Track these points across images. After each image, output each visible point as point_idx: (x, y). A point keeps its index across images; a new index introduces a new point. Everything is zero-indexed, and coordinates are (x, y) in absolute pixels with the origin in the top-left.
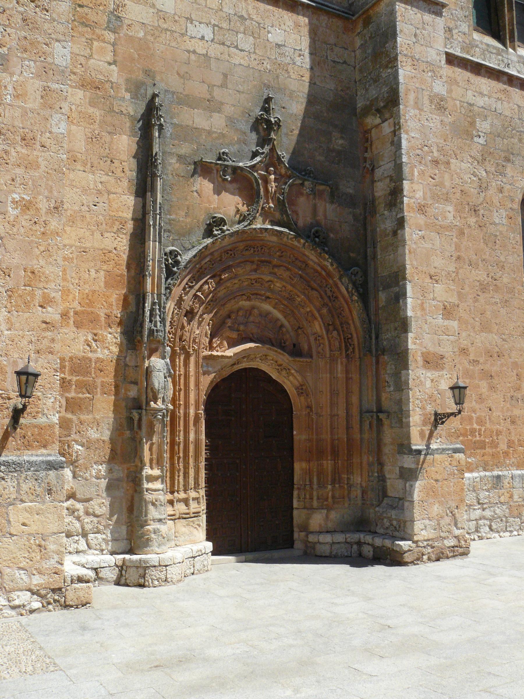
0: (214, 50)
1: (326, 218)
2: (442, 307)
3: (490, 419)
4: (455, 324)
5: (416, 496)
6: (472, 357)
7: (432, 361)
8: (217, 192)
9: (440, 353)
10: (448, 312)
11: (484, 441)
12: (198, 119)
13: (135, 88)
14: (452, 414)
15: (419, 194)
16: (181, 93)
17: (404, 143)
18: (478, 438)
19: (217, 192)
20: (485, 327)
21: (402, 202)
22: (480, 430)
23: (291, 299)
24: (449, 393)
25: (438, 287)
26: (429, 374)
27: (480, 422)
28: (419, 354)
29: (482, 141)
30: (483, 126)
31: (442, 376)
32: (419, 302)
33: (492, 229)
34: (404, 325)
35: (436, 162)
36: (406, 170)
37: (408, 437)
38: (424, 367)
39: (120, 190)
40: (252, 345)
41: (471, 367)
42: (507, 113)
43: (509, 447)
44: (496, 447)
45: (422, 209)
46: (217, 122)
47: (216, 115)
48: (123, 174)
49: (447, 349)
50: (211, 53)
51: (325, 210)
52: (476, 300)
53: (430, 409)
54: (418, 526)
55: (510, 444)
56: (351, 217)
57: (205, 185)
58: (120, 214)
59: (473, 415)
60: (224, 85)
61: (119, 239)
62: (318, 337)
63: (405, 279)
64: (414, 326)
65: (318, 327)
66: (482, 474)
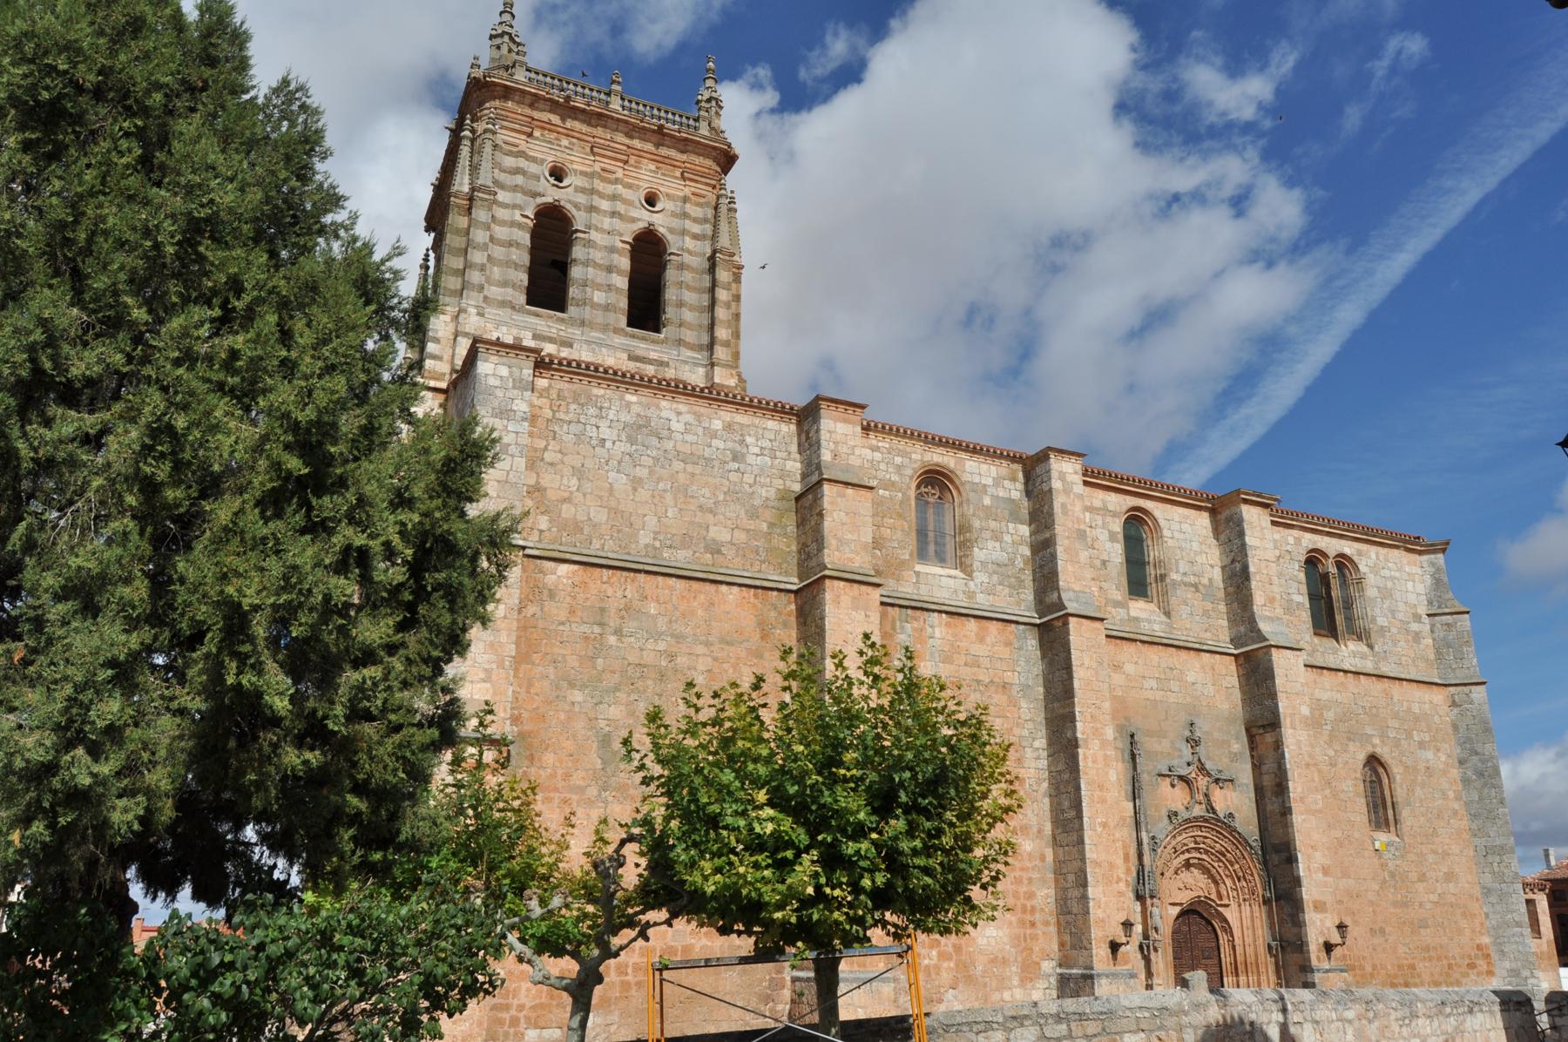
0: (1159, 695)
4: (1329, 879)
7: (1320, 907)
10: (1326, 871)
13: (1120, 729)
25: (1318, 854)
33: (1342, 796)
34: (1297, 882)
35: (1308, 765)
45: (1302, 799)
49: (1328, 899)
53: (1321, 941)
55: (1374, 967)
64: (1304, 882)
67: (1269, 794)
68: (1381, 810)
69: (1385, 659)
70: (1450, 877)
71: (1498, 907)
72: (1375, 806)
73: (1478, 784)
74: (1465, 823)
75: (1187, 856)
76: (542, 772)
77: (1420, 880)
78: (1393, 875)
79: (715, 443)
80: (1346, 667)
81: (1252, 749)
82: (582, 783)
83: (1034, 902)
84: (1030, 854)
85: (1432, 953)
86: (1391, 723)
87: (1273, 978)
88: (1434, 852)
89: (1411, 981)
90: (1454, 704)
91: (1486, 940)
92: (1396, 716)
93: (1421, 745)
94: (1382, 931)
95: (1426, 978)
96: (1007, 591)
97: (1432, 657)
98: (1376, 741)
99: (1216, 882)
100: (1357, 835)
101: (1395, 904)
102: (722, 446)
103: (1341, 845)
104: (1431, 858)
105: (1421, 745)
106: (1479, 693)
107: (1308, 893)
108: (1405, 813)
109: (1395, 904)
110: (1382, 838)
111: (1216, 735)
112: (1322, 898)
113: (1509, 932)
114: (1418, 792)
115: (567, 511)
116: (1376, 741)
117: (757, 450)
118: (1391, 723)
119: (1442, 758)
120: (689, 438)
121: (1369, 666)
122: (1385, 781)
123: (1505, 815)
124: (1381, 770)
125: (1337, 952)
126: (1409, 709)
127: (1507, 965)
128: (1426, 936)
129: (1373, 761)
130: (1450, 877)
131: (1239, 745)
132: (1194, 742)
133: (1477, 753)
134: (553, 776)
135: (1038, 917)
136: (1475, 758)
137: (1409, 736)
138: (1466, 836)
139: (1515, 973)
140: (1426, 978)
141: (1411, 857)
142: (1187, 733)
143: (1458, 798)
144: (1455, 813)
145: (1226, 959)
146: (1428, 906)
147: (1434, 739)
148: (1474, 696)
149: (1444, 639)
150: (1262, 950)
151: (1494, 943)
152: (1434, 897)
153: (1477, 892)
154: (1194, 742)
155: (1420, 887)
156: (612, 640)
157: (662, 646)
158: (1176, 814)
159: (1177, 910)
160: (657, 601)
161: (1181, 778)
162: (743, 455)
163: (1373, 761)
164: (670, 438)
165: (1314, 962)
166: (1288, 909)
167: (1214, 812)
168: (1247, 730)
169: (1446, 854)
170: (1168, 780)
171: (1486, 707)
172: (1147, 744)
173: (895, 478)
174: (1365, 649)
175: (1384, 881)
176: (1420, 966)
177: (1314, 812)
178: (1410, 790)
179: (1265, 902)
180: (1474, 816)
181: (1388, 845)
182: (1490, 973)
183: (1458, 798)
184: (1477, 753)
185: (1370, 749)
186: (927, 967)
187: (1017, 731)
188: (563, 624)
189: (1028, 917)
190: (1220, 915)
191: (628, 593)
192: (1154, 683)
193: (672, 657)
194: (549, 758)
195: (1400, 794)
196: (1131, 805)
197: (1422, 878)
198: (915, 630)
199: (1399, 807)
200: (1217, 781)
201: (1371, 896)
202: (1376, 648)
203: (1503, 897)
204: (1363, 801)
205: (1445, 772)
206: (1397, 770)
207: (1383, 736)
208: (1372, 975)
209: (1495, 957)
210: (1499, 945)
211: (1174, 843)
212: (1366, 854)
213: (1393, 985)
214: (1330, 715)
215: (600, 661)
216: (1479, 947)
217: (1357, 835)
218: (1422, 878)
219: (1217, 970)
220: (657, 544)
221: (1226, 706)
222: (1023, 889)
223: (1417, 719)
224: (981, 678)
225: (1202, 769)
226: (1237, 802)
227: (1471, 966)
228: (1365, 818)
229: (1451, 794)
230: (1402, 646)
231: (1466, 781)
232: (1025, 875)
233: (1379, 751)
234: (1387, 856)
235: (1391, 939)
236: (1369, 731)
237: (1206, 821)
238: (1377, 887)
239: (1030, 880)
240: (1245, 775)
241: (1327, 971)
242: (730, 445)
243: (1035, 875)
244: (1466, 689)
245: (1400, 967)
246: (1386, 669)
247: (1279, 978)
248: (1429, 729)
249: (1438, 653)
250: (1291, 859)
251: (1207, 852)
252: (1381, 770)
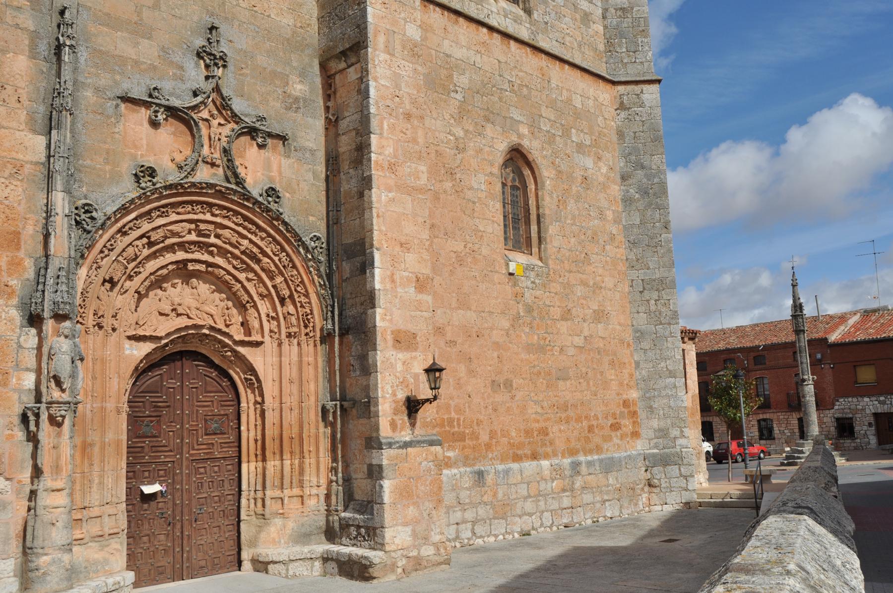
1: (280, 173)
2: (415, 279)
3: (469, 407)
4: (427, 298)
5: (387, 498)
6: (449, 336)
9: (413, 331)
10: (421, 284)
11: (464, 432)
14: (427, 400)
15: (389, 151)
16: (100, 11)
17: (372, 92)
18: (456, 429)
20: (463, 304)
21: (370, 160)
22: (459, 419)
24: (423, 377)
25: (410, 258)
26: (400, 356)
27: (459, 410)
28: (389, 332)
29: (459, 96)
30: (463, 80)
31: (415, 358)
32: (389, 273)
33: (469, 194)
34: (371, 300)
35: (408, 116)
36: (374, 123)
37: (377, 429)
38: (394, 347)
39: (14, 124)
41: (448, 349)
42: (486, 68)
43: (491, 438)
44: (477, 438)
46: (147, 51)
48: (18, 105)
49: (421, 328)
51: (280, 167)
52: (452, 272)
53: (401, 395)
54: (388, 534)
55: (492, 434)
56: (310, 175)
58: (14, 155)
59: (451, 402)
61: (12, 187)
63: (372, 246)
64: (382, 300)
66: (462, 470)
67: (345, 166)
68: (522, 224)
69: (545, 31)
70: (600, 316)
71: (650, 354)
72: (516, 220)
73: (641, 205)
74: (622, 252)
75: (181, 255)
77: (564, 318)
78: (529, 310)
80: (494, 23)
81: (328, 97)
85: (571, 413)
86: (545, 112)
87: (325, 459)
88: (584, 284)
89: (541, 450)
90: (622, 107)
91: (634, 394)
92: (552, 104)
93: (580, 147)
94: (508, 384)
95: (560, 445)
97: (601, 47)
98: (524, 130)
99: (242, 307)
100: (485, 251)
101: (529, 348)
103: (461, 261)
104: (579, 291)
105: (580, 147)
106: (651, 94)
107: (385, 319)
108: (552, 230)
109: (529, 348)
110: (519, 261)
111: (262, 60)
112: (411, 327)
113: (661, 383)
114: (571, 205)
116: (524, 130)
118: (545, 112)
119: (603, 167)
121: (524, 33)
122: (531, 187)
123: (668, 241)
124: (527, 172)
125: (426, 413)
126: (569, 101)
127: (655, 423)
128: (566, 391)
129: (518, 159)
130: (600, 316)
131: (306, 86)
132: (211, 58)
133: (643, 167)
136: (640, 173)
137: (566, 133)
138: (622, 267)
139: (662, 433)
140: (560, 445)
141: (555, 287)
142: (200, 42)
143: (617, 221)
144: (613, 237)
145: (249, 433)
146: (571, 351)
147: (595, 144)
148: (645, 97)
149: (617, 27)
150: (312, 416)
151: (644, 398)
152: (579, 341)
153: (628, 336)
154: (211, 58)
155: (563, 326)
158: (151, 172)
159: (147, 348)
161: (173, 112)
163: (518, 159)
165: (385, 431)
166: (356, 349)
167: (240, 182)
168: (323, 66)
169: (598, 287)
170: (144, 114)
171: (658, 111)
172: (98, 38)
174: (522, 13)
175: (518, 317)
176: (554, 430)
177: (412, 191)
178: (562, 202)
179: (323, 340)
180: (633, 244)
181: (528, 268)
182: (636, 434)
183: (617, 221)
184: (643, 167)
185: (515, 139)
190: (242, 360)
195: (549, 204)
196: (42, 141)
197: (567, 315)
199: (546, 221)
200: (252, 132)
201: (497, 336)
202: (535, 15)
203: (657, 340)
204: (499, 206)
205: (604, 187)
206: (546, 173)
207: (534, 127)
208: (488, 446)
209: (642, 414)
210: (647, 398)
211: (146, 227)
212: (496, 277)
213: (517, 458)
214: (463, 80)
216: (626, 404)
217: (485, 251)
218: (567, 315)
219: (232, 452)
221: (287, 20)
223: (577, 115)
225: (223, 106)
226: (291, 176)
227: (615, 427)
228: (499, 230)
229: (610, 215)
230: (567, 23)
231: (627, 201)
233: (526, 143)
234: (525, 283)
235: (519, 395)
236: (516, 114)
237: (220, 194)
238: (506, 324)
240: (311, 133)
241: (406, 445)
244: (637, 88)
245: (528, 433)
246: (543, 44)
247: (335, 460)
248: (591, 133)
249: (609, 43)
250: (365, 266)
251: (223, 253)
252: (527, 172)
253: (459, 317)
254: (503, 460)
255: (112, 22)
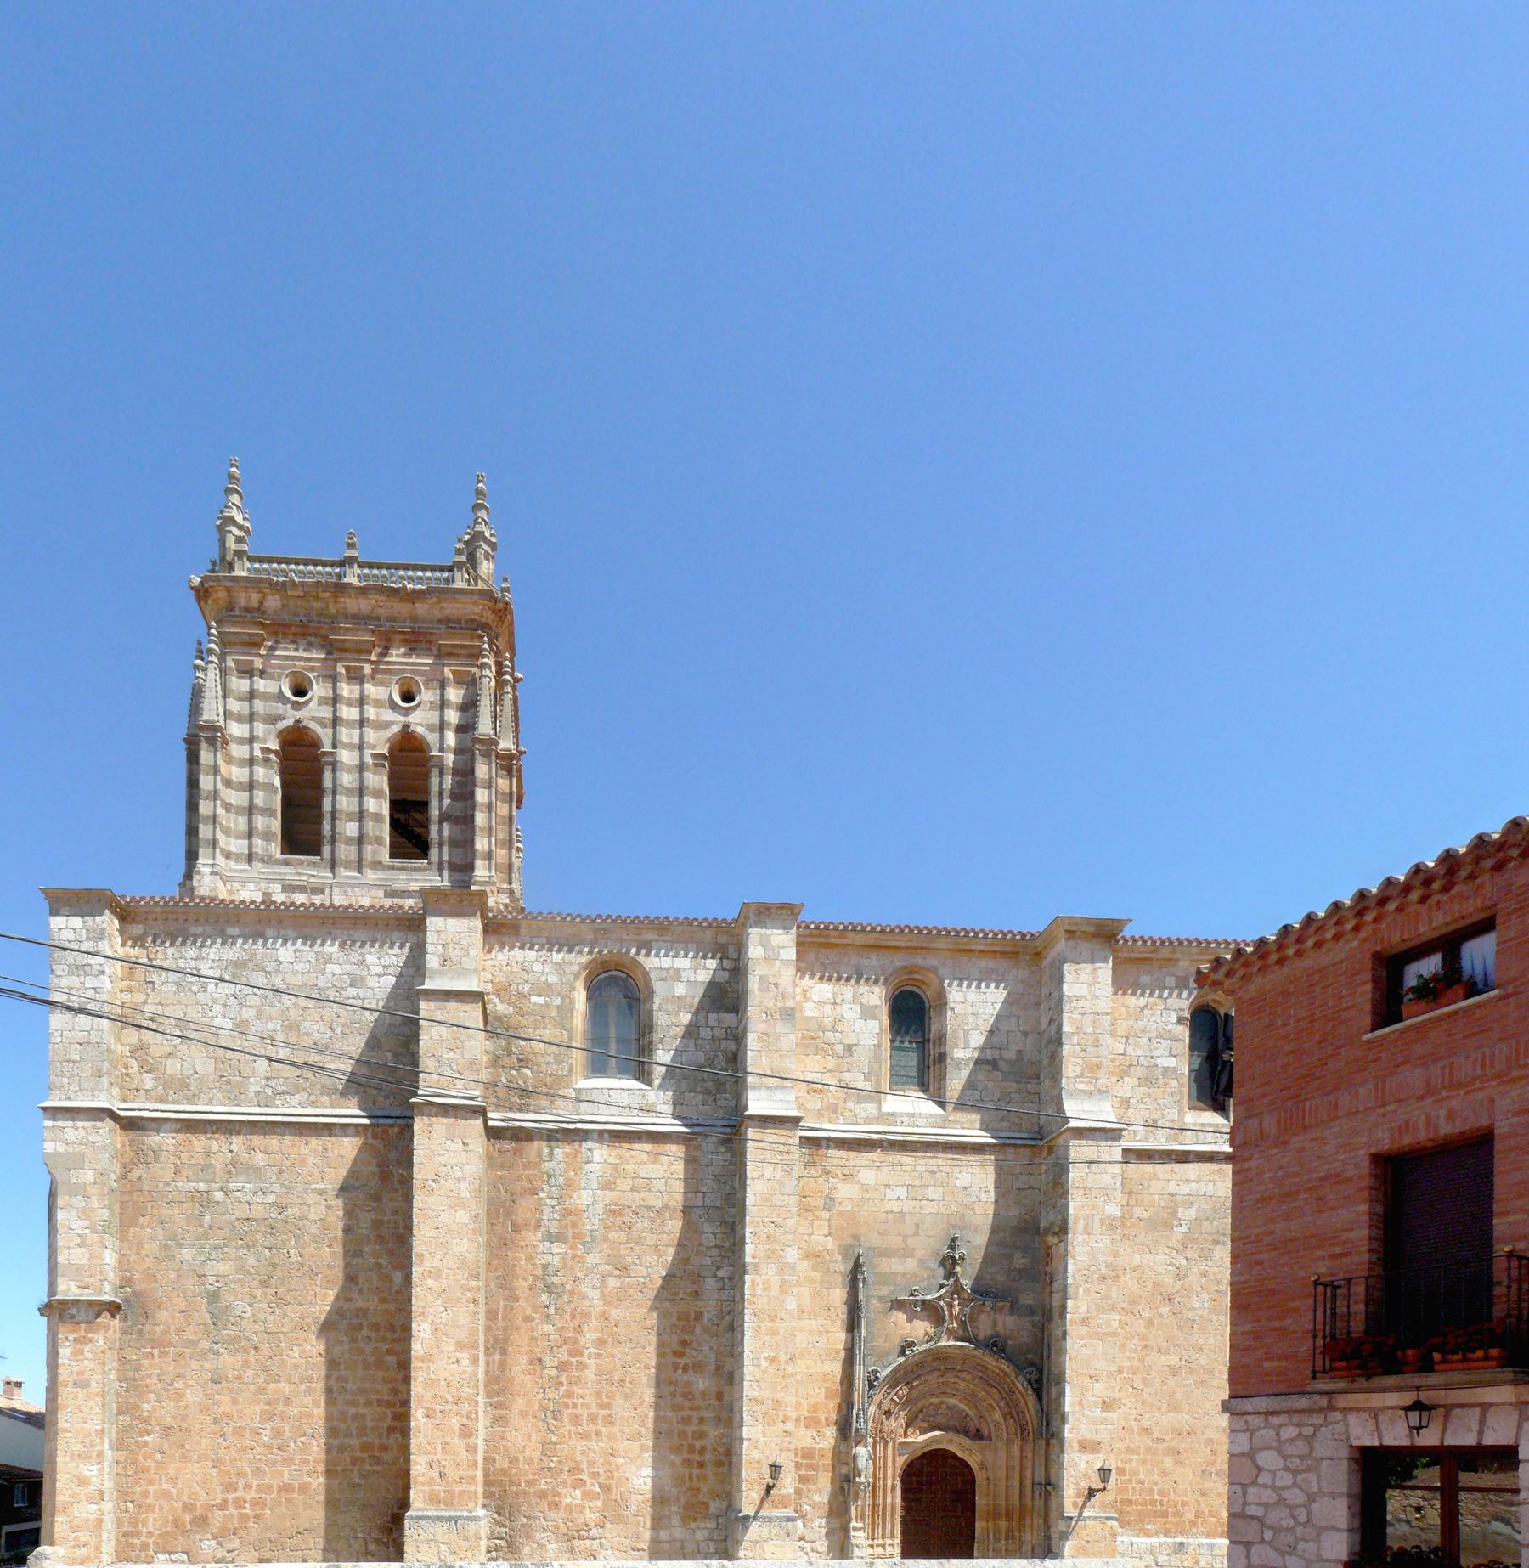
0: (908, 1206)
6: (1156, 1435)
8: (910, 1320)
12: (895, 1266)
13: (846, 1251)
19: (910, 1320)
20: (1174, 1408)
23: (974, 1395)
27: (1162, 1493)
40: (938, 1433)
44: (1181, 1516)
46: (911, 1265)
47: (909, 1260)
50: (906, 1210)
52: (1164, 1383)
57: (900, 1317)
60: (916, 1234)
62: (997, 1424)
65: (997, 1415)
66: (1163, 1540)
76: (157, 1329)
79: (330, 968)
82: (195, 1338)
83: (706, 1442)
84: (704, 1394)
96: (700, 1097)
102: (338, 970)
115: (173, 1067)
117: (379, 969)
120: (299, 967)
134: (166, 1332)
135: (708, 1456)
156: (219, 1196)
157: (271, 1198)
160: (265, 1152)
162: (363, 978)
164: (278, 971)
173: (553, 979)
186: (569, 1506)
187: (696, 1261)
188: (168, 1184)
189: (697, 1457)
191: (234, 1147)
192: (902, 1192)
193: (282, 1207)
194: (163, 1315)
198: (567, 1155)
208: (1193, 1523)
215: (207, 1218)
220: (269, 1091)
222: (690, 1429)
224: (651, 1203)
232: (695, 1414)
239: (702, 1420)
242: (347, 967)
243: (708, 1415)
253: (1168, 1420)
254: (1208, 1535)
255: (887, 1253)
